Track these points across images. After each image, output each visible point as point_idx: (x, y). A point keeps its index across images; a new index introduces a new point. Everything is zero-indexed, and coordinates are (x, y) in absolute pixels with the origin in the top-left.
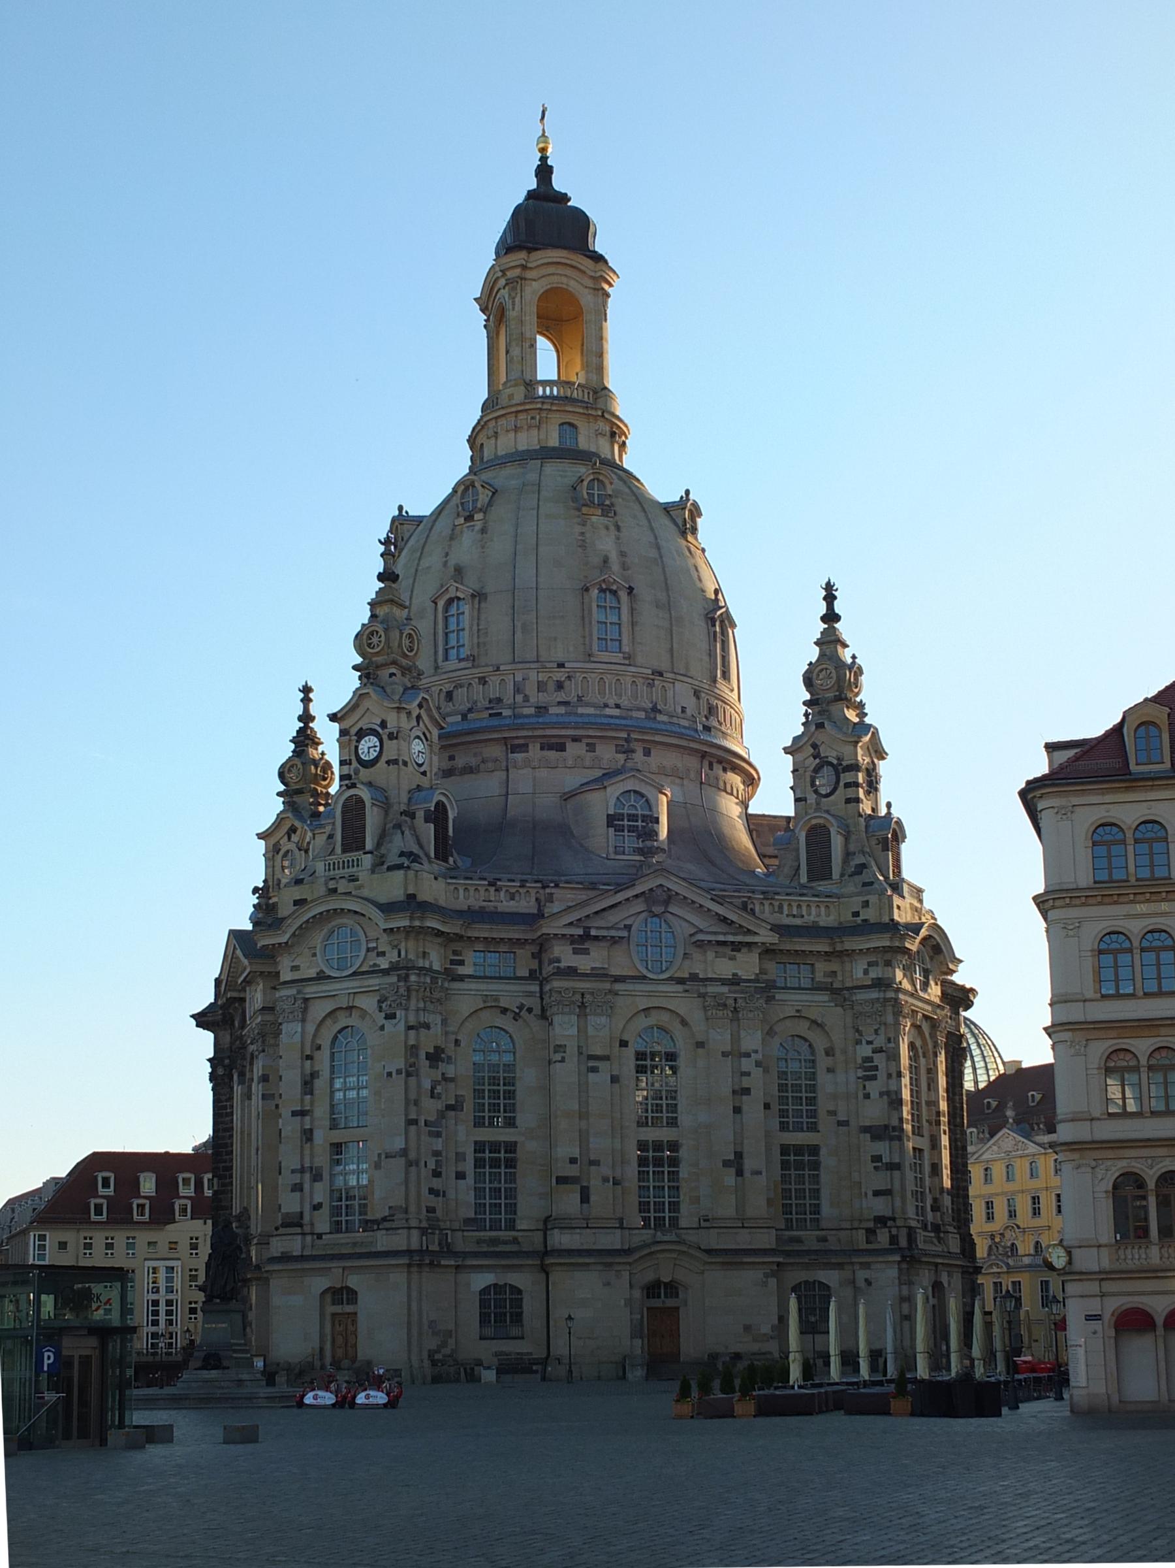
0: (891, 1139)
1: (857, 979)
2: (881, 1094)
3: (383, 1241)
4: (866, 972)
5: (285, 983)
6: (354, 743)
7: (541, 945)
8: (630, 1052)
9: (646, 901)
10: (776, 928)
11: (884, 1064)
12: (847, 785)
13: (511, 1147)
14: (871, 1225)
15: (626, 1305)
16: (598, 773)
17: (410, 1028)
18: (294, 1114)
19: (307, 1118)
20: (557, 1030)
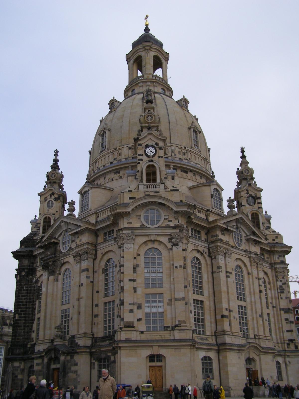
0: (291, 313)
1: (276, 260)
2: (287, 298)
3: (177, 335)
4: (278, 258)
5: (125, 228)
6: (144, 149)
7: (208, 231)
8: (234, 273)
9: (236, 222)
10: (266, 239)
11: (287, 288)
12: (259, 203)
13: (202, 302)
14: (287, 342)
15: (244, 366)
16: (196, 184)
17: (184, 250)
18: (130, 280)
19: (135, 282)
20: (220, 261)
